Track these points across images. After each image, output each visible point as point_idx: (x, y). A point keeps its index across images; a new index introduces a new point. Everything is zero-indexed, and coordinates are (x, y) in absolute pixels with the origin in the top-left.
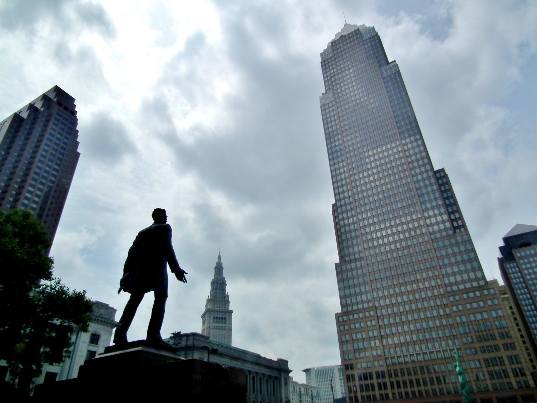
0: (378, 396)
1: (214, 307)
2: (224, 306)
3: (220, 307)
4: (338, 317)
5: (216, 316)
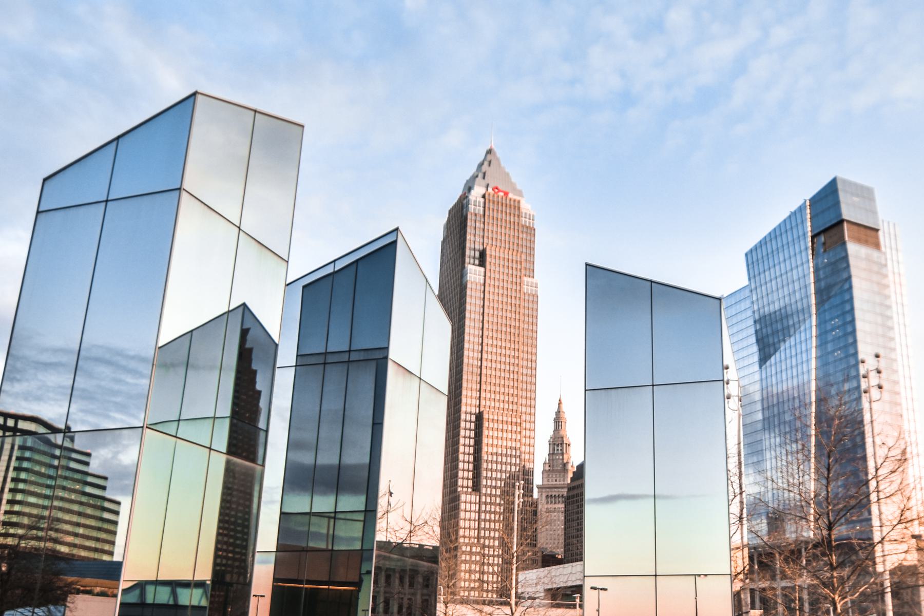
2: (562, 479)
3: (556, 481)
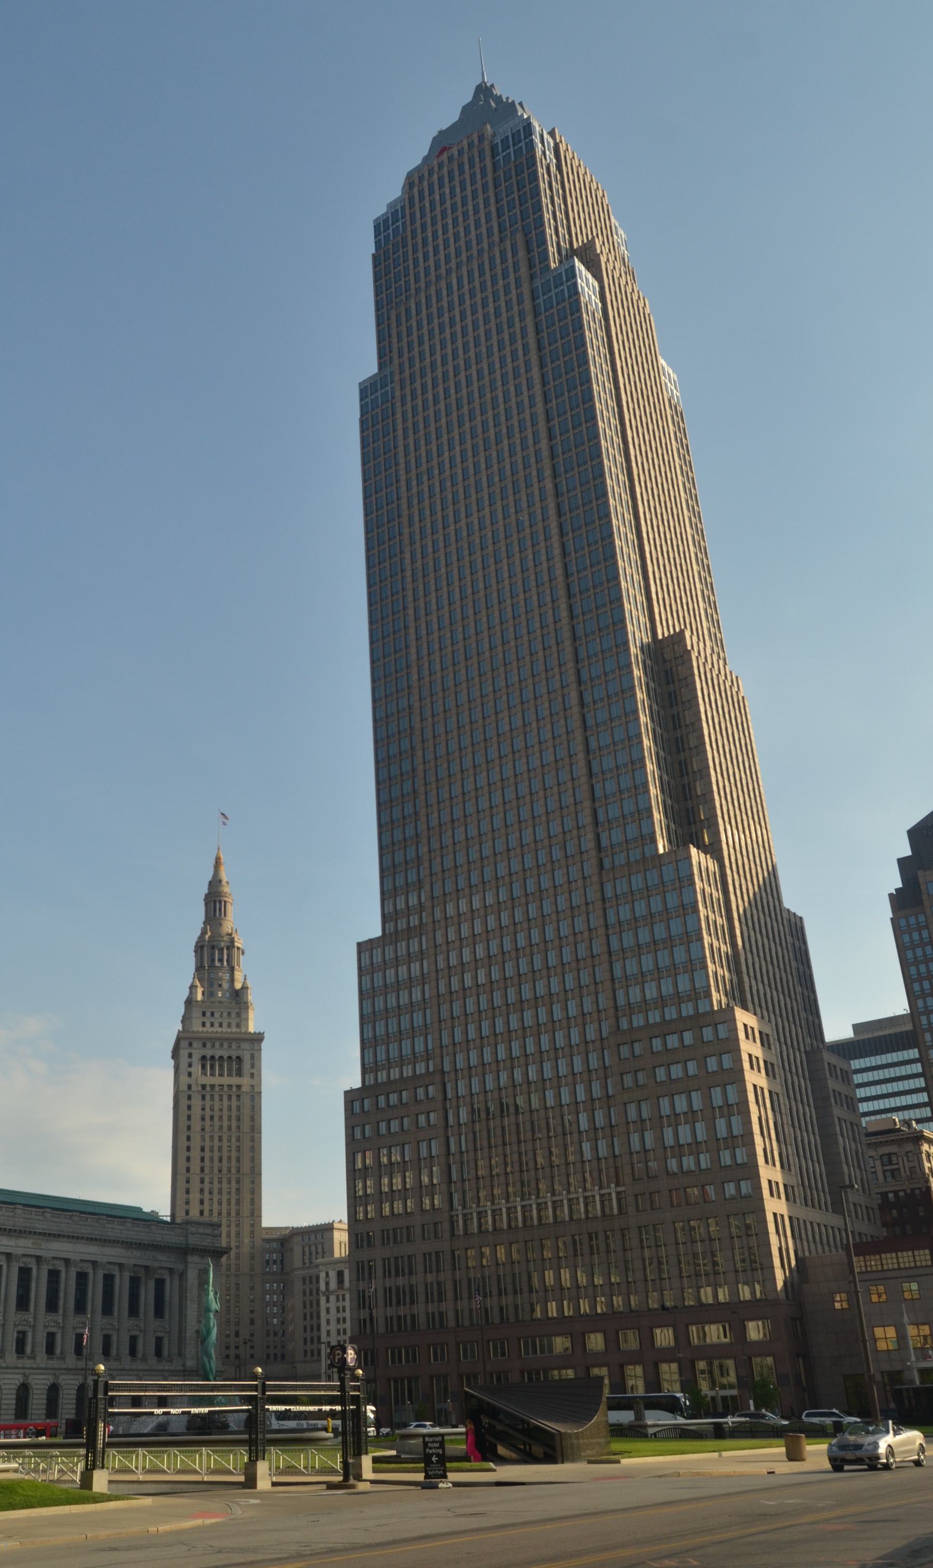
0: (422, 1319)
1: (204, 1025)
2: (234, 1023)
3: (221, 1025)
4: (352, 1102)
5: (208, 1053)
